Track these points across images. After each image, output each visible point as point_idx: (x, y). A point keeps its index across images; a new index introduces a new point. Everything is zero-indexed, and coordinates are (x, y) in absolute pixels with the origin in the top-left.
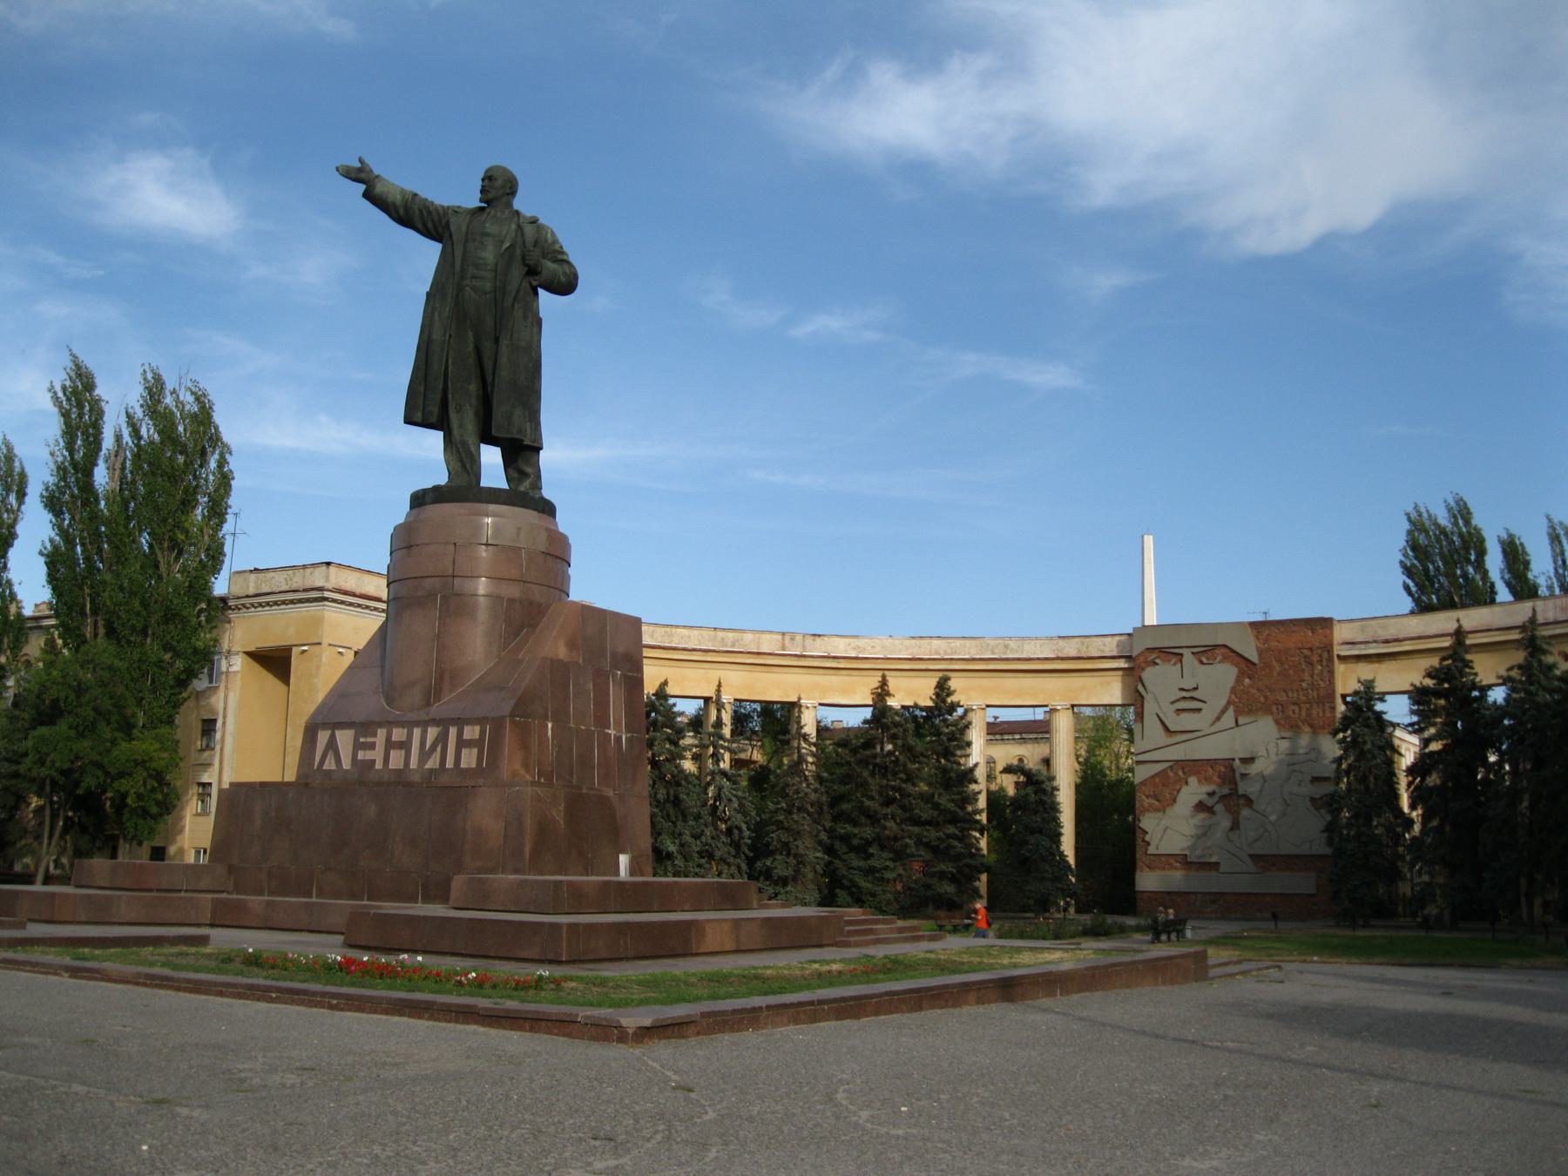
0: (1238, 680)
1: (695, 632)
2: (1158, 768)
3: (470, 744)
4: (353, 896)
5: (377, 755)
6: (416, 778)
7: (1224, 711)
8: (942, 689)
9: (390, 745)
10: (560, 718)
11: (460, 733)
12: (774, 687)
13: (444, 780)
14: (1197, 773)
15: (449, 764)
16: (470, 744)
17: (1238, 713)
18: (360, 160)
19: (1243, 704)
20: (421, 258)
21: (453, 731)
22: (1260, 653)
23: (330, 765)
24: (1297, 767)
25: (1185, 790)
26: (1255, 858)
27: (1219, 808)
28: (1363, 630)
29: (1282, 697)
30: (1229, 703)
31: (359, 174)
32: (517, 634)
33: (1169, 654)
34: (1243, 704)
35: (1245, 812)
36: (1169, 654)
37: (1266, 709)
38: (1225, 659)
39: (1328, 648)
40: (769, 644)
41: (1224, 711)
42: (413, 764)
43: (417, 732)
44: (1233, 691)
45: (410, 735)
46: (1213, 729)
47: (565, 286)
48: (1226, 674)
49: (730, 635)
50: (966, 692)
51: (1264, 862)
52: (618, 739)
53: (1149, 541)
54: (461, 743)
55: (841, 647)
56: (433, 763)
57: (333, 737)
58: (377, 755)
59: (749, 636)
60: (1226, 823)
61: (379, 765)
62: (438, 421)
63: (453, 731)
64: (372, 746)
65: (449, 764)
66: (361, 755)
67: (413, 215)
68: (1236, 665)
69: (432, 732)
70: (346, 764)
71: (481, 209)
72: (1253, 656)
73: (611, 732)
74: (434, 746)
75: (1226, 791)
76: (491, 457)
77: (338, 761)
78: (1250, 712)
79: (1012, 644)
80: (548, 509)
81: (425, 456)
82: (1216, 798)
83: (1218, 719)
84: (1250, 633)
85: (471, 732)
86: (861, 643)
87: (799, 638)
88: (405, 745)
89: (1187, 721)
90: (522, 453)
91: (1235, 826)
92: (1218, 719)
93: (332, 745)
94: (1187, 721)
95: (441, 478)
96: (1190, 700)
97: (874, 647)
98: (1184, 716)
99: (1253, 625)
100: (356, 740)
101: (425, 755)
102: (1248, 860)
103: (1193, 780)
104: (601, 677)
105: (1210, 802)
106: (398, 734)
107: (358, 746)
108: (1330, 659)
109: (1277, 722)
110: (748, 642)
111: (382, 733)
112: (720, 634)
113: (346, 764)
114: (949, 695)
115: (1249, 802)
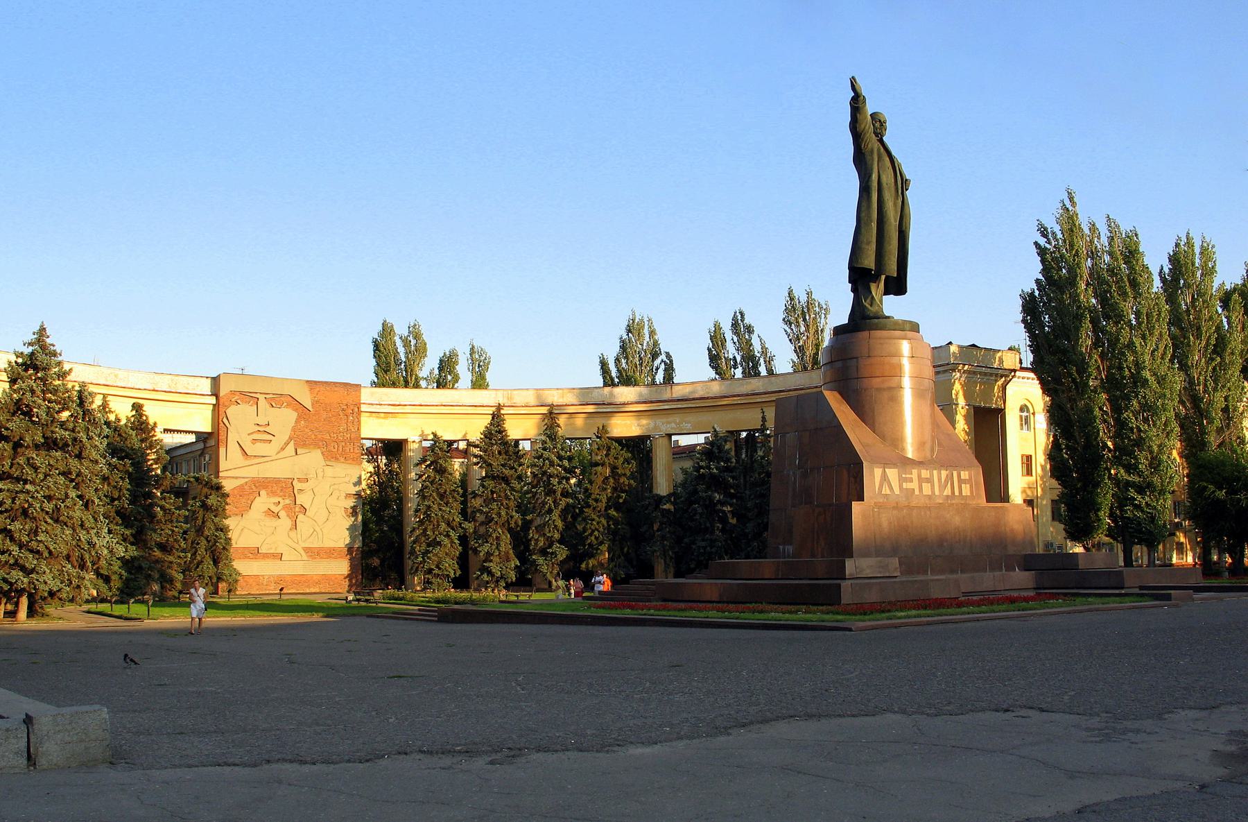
2: (243, 481)
3: (965, 481)
5: (914, 485)
7: (287, 444)
9: (921, 480)
11: (959, 476)
14: (265, 487)
15: (957, 493)
16: (965, 481)
19: (300, 441)
21: (955, 474)
23: (886, 490)
25: (258, 499)
26: (307, 550)
30: (291, 439)
33: (250, 397)
34: (300, 441)
35: (301, 517)
36: (250, 397)
37: (315, 444)
38: (288, 405)
39: (358, 405)
41: (287, 444)
42: (937, 493)
44: (294, 429)
45: (932, 475)
50: (153, 413)
51: (315, 553)
54: (961, 481)
56: (947, 492)
57: (884, 474)
58: (914, 485)
61: (917, 492)
64: (911, 480)
65: (957, 493)
66: (905, 485)
68: (296, 410)
70: (897, 491)
72: (308, 404)
75: (287, 502)
77: (891, 488)
78: (304, 445)
82: (281, 506)
84: (306, 389)
85: (965, 475)
88: (929, 480)
89: (260, 449)
92: (283, 449)
93: (884, 477)
94: (260, 449)
96: (264, 432)
98: (258, 444)
100: (900, 476)
101: (942, 488)
103: (263, 493)
105: (275, 509)
106: (925, 473)
107: (902, 480)
108: (360, 412)
113: (897, 491)
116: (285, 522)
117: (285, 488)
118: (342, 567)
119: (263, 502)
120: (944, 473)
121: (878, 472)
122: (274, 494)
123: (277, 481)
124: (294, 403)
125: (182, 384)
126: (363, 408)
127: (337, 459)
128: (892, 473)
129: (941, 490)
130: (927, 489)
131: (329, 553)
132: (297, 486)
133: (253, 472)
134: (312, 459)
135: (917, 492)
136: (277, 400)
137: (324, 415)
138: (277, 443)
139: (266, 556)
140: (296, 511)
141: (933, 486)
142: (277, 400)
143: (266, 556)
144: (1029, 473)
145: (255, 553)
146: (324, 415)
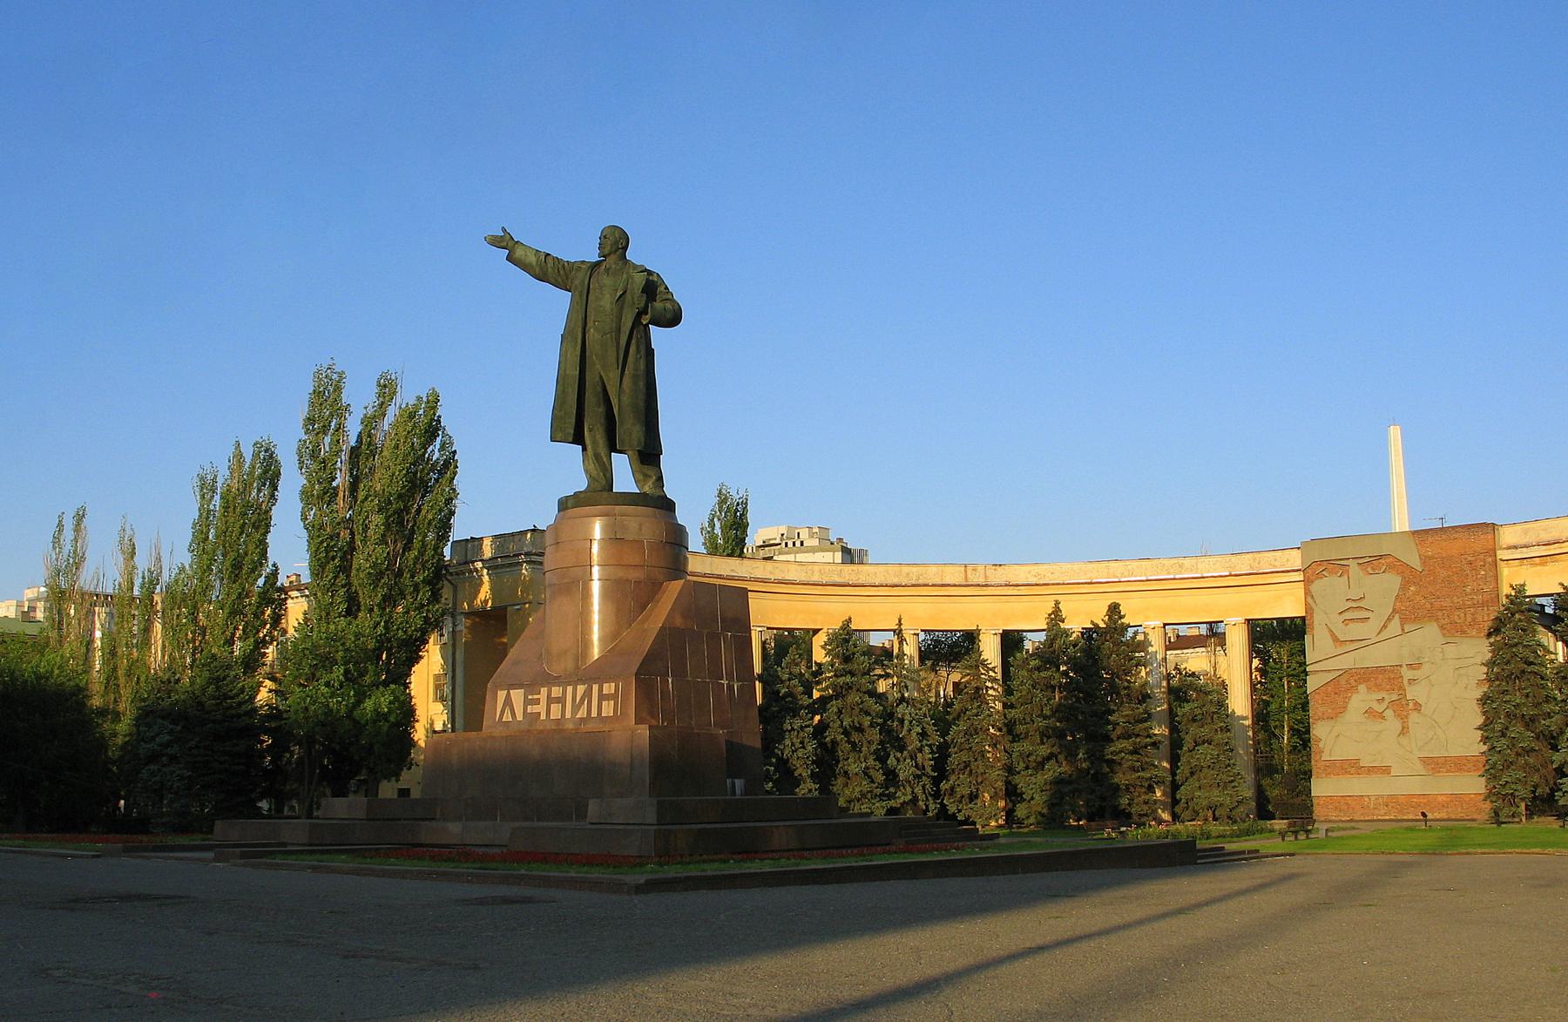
0: (1404, 587)
1: (881, 568)
3: (608, 697)
4: (526, 819)
5: (541, 708)
6: (571, 726)
8: (1114, 609)
9: (550, 700)
10: (679, 674)
11: (601, 690)
12: (954, 617)
13: (590, 726)
15: (594, 714)
16: (608, 697)
17: (1403, 621)
18: (504, 230)
19: (1408, 613)
20: (557, 304)
21: (595, 687)
22: (1424, 563)
23: (507, 717)
24: (1462, 671)
26: (1426, 761)
27: (1389, 713)
28: (1526, 532)
29: (1447, 603)
31: (504, 242)
32: (643, 607)
37: (1431, 616)
40: (953, 575)
42: (568, 715)
43: (570, 689)
45: (564, 692)
46: (1381, 637)
47: (672, 318)
48: (1391, 582)
49: (914, 569)
51: (1435, 765)
52: (730, 688)
53: (1395, 433)
54: (602, 697)
55: (1022, 574)
56: (582, 713)
57: (508, 694)
59: (934, 569)
60: (1397, 725)
61: (543, 717)
62: (578, 439)
63: (595, 687)
64: (537, 702)
65: (594, 714)
67: (549, 271)
69: (581, 689)
70: (520, 717)
71: (598, 264)
72: (1415, 563)
73: (725, 682)
74: (582, 700)
75: (1395, 697)
76: (622, 466)
77: (513, 714)
78: (1416, 619)
79: (1187, 562)
80: (669, 506)
81: (569, 468)
82: (1385, 705)
83: (1385, 626)
85: (609, 688)
86: (1042, 569)
87: (981, 568)
88: (561, 700)
89: (1357, 630)
90: (649, 456)
91: (1404, 731)
92: (1385, 626)
94: (1357, 630)
95: (580, 483)
96: (1356, 610)
97: (1047, 573)
98: (1351, 625)
99: (1414, 533)
102: (1418, 763)
103: (1362, 688)
104: (714, 637)
105: (1379, 708)
106: (556, 691)
107: (527, 702)
109: (1442, 628)
110: (932, 574)
111: (544, 691)
112: (905, 569)
113: (520, 717)
114: (1121, 617)
115: (1418, 707)
116: (1392, 724)
117: (1385, 678)
118: (1474, 785)
119: (1361, 699)
120: (581, 689)
121: (502, 695)
122: (1379, 687)
123: (1381, 670)
124: (1397, 566)
125: (1267, 562)
126: (1501, 554)
127: (1463, 632)
128: (517, 695)
129: (574, 712)
130: (556, 711)
131: (1458, 765)
132: (1407, 674)
133: (1346, 662)
134: (1428, 635)
135: (543, 717)
136: (1375, 562)
137: (1443, 573)
138: (1375, 623)
139: (1372, 770)
140: (1403, 708)
141: (564, 707)
142: (1375, 562)
143: (1372, 770)
144: (1170, 646)
145: (1351, 767)
146: (1443, 573)
